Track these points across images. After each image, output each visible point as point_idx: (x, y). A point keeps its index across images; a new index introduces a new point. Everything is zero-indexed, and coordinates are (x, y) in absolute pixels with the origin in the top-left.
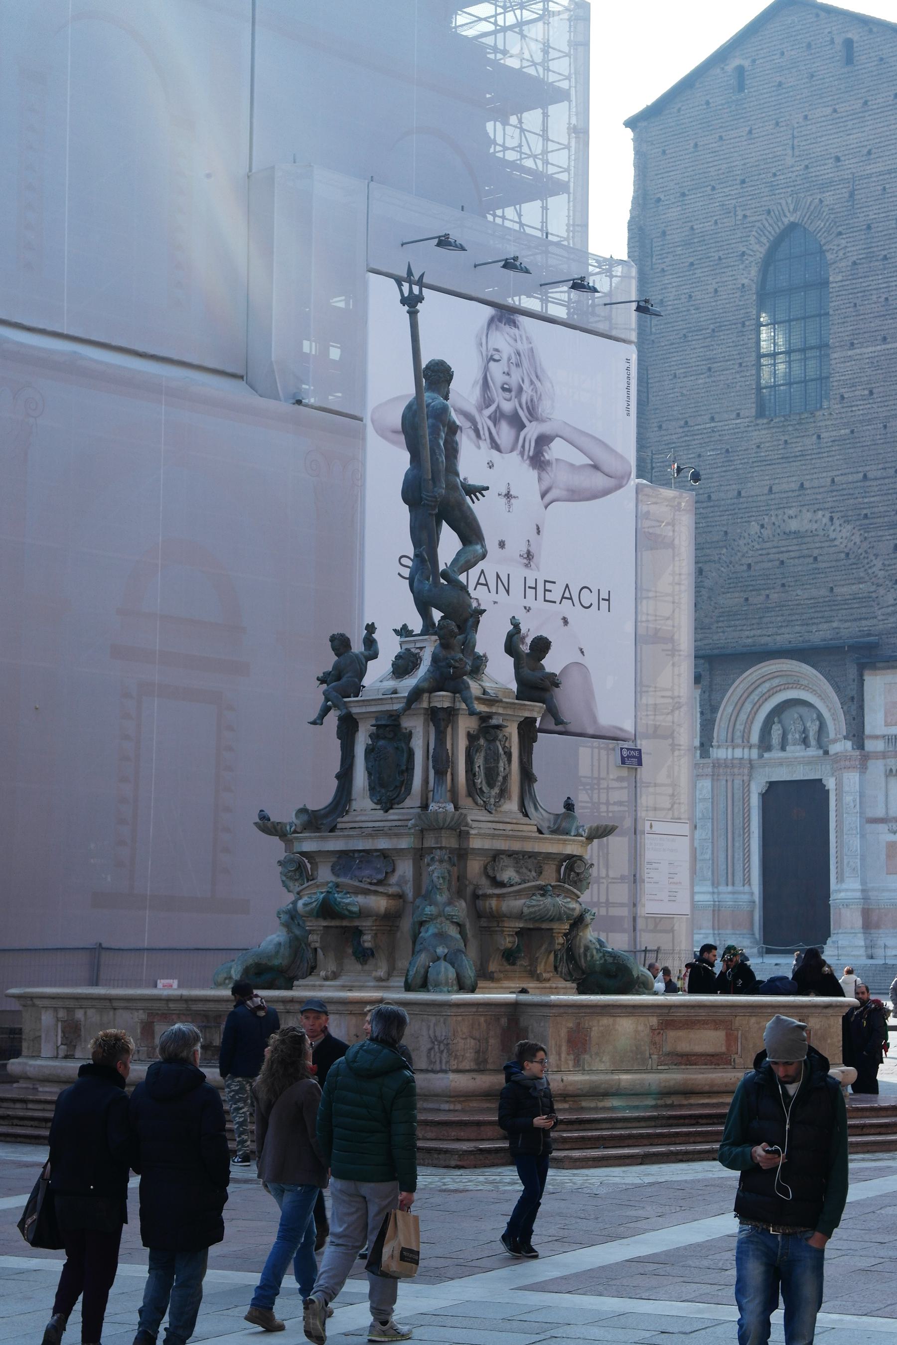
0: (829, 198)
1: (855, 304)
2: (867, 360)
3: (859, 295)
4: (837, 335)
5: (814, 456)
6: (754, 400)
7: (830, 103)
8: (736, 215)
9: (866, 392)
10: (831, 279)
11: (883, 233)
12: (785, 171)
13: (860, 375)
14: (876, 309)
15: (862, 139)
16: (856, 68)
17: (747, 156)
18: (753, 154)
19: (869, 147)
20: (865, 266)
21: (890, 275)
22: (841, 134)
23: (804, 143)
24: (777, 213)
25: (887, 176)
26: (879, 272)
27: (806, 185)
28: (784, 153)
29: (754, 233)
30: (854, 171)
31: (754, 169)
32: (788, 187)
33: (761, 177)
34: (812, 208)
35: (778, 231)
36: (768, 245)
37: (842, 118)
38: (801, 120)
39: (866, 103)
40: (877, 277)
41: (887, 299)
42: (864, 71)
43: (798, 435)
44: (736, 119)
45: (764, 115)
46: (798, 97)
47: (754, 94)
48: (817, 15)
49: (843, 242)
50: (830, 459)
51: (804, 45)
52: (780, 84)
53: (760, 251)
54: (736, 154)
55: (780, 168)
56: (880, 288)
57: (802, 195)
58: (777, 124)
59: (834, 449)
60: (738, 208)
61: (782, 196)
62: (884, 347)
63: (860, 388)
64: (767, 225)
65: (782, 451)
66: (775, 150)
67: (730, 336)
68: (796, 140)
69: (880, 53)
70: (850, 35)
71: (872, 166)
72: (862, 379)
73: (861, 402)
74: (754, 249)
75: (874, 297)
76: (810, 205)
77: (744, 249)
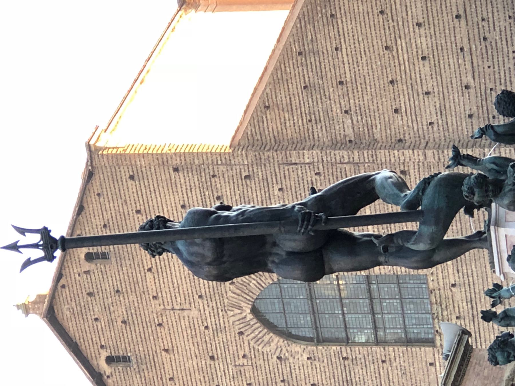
5: (472, 291)
6: (418, 349)
7: (143, 274)
8: (243, 365)
12: (204, 317)
17: (189, 355)
18: (187, 348)
22: (171, 264)
23: (178, 299)
27: (217, 298)
28: (186, 318)
29: (260, 348)
31: (201, 348)
32: (218, 314)
34: (238, 291)
35: (258, 325)
36: (271, 334)
37: (156, 263)
38: (157, 302)
43: (451, 306)
44: (155, 365)
45: (151, 338)
46: (136, 305)
47: (132, 346)
48: (63, 286)
50: (475, 274)
51: (89, 299)
52: (124, 322)
53: (277, 341)
54: (187, 365)
55: (200, 322)
57: (226, 301)
58: (160, 325)
59: (465, 271)
60: (237, 363)
61: (226, 320)
64: (253, 335)
65: (467, 321)
66: (184, 327)
67: (356, 371)
68: (176, 307)
69: (99, 227)
70: (82, 256)
74: (275, 347)
76: (235, 293)
77: (275, 357)
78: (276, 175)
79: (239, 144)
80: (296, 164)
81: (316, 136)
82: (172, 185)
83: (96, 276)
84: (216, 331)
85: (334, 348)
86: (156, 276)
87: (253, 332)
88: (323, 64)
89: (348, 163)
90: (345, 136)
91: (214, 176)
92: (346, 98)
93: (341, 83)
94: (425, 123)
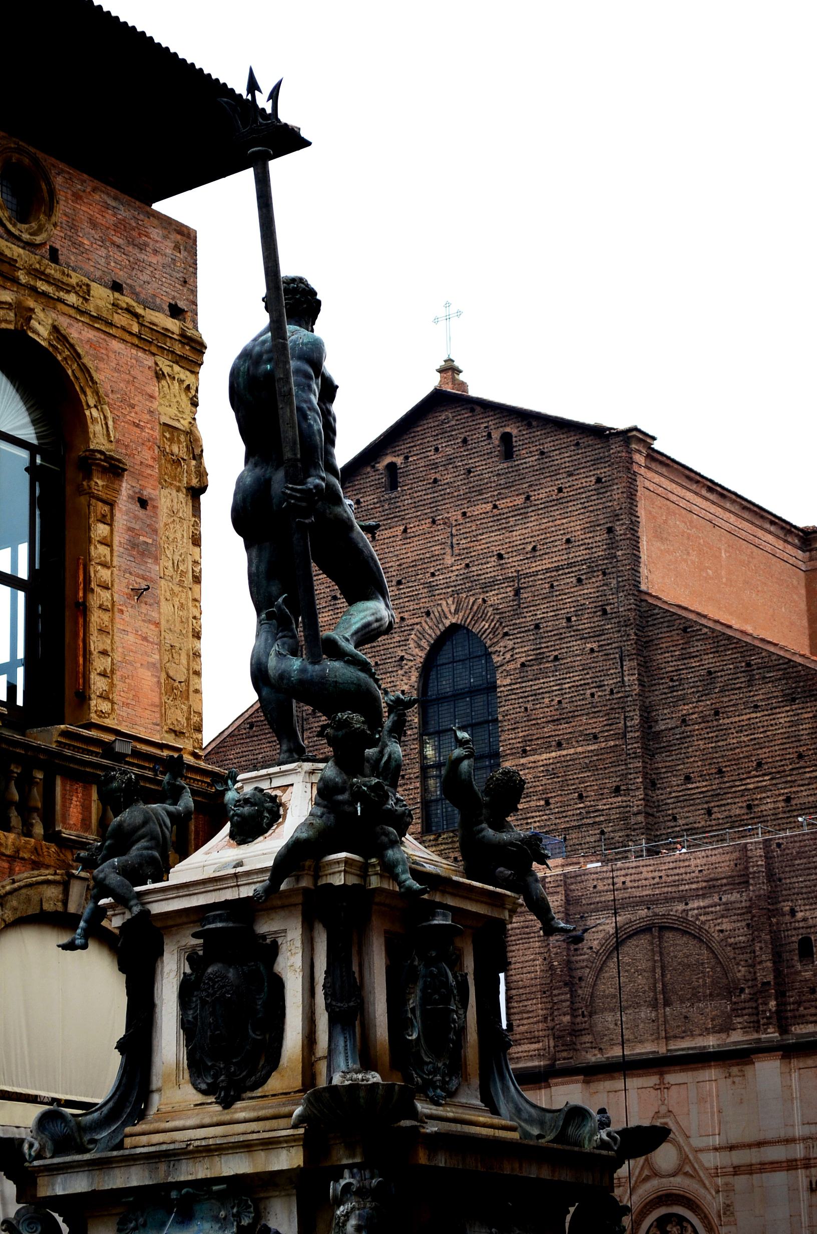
0: (493, 598)
1: (526, 709)
2: (542, 768)
3: (530, 698)
4: (508, 742)
7: (490, 499)
9: (542, 803)
10: (498, 682)
11: (553, 633)
13: (534, 784)
14: (549, 714)
15: (526, 536)
16: (516, 463)
17: (402, 557)
18: (409, 555)
19: (533, 544)
20: (535, 668)
21: (562, 677)
23: (464, 541)
24: (437, 614)
25: (555, 573)
26: (550, 675)
28: (442, 552)
30: (519, 568)
32: (449, 587)
33: (419, 577)
34: (475, 608)
35: (438, 633)
38: (459, 517)
39: (528, 498)
40: (548, 680)
41: (560, 702)
42: (524, 466)
45: (419, 513)
47: (409, 492)
49: (510, 644)
51: (460, 440)
52: (435, 481)
53: (420, 655)
54: (390, 555)
55: (439, 567)
56: (553, 691)
57: (464, 595)
58: (434, 522)
62: (559, 753)
63: (535, 798)
70: (508, 430)
71: (538, 563)
72: (537, 789)
73: (538, 814)
74: (414, 653)
75: (547, 700)
76: (473, 605)
78: (608, 644)
79: (642, 601)
80: (622, 667)
81: (654, 688)
82: (593, 527)
83: (485, 446)
84: (430, 587)
85: (416, 720)
86: (490, 514)
87: (430, 627)
88: (737, 692)
89: (626, 727)
90: (657, 721)
91: (604, 574)
92: (700, 720)
93: (717, 713)
94: (675, 811)
